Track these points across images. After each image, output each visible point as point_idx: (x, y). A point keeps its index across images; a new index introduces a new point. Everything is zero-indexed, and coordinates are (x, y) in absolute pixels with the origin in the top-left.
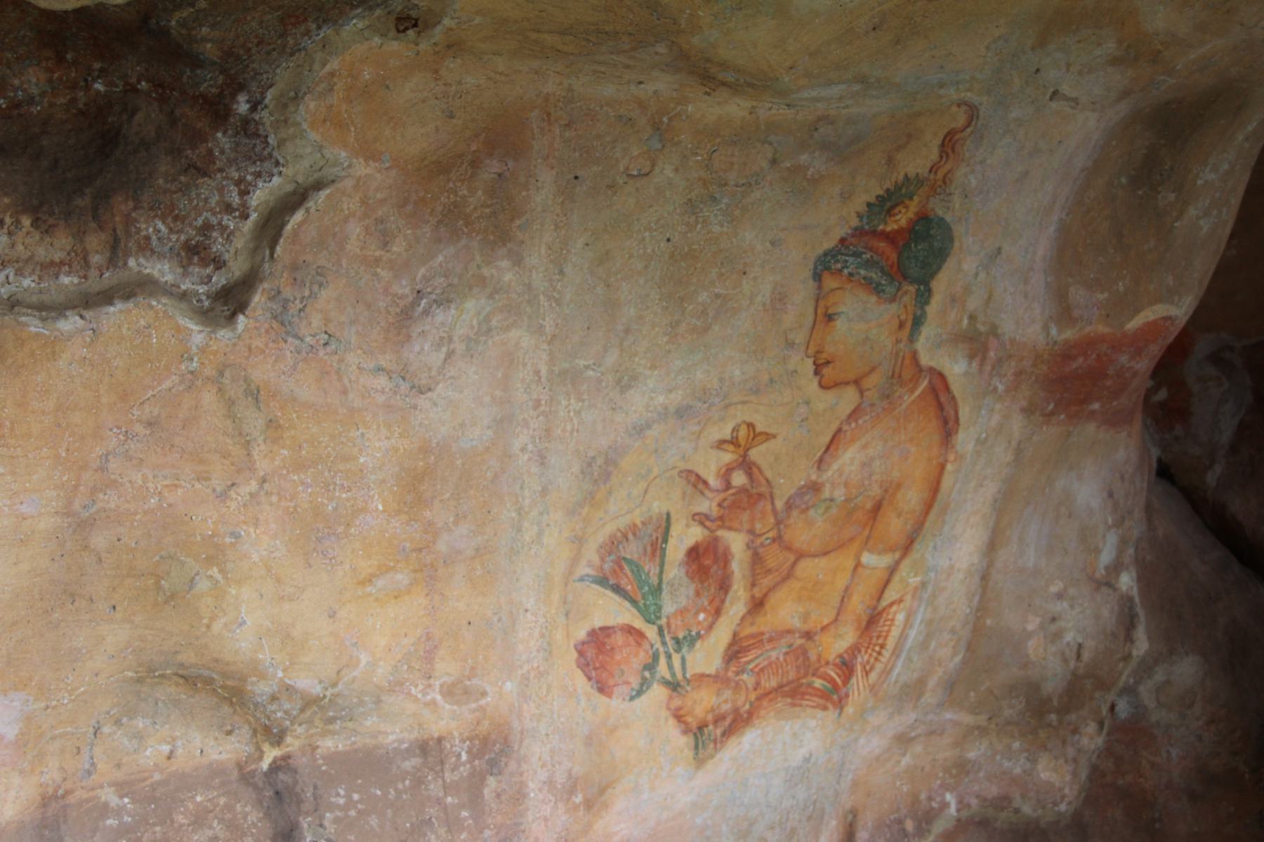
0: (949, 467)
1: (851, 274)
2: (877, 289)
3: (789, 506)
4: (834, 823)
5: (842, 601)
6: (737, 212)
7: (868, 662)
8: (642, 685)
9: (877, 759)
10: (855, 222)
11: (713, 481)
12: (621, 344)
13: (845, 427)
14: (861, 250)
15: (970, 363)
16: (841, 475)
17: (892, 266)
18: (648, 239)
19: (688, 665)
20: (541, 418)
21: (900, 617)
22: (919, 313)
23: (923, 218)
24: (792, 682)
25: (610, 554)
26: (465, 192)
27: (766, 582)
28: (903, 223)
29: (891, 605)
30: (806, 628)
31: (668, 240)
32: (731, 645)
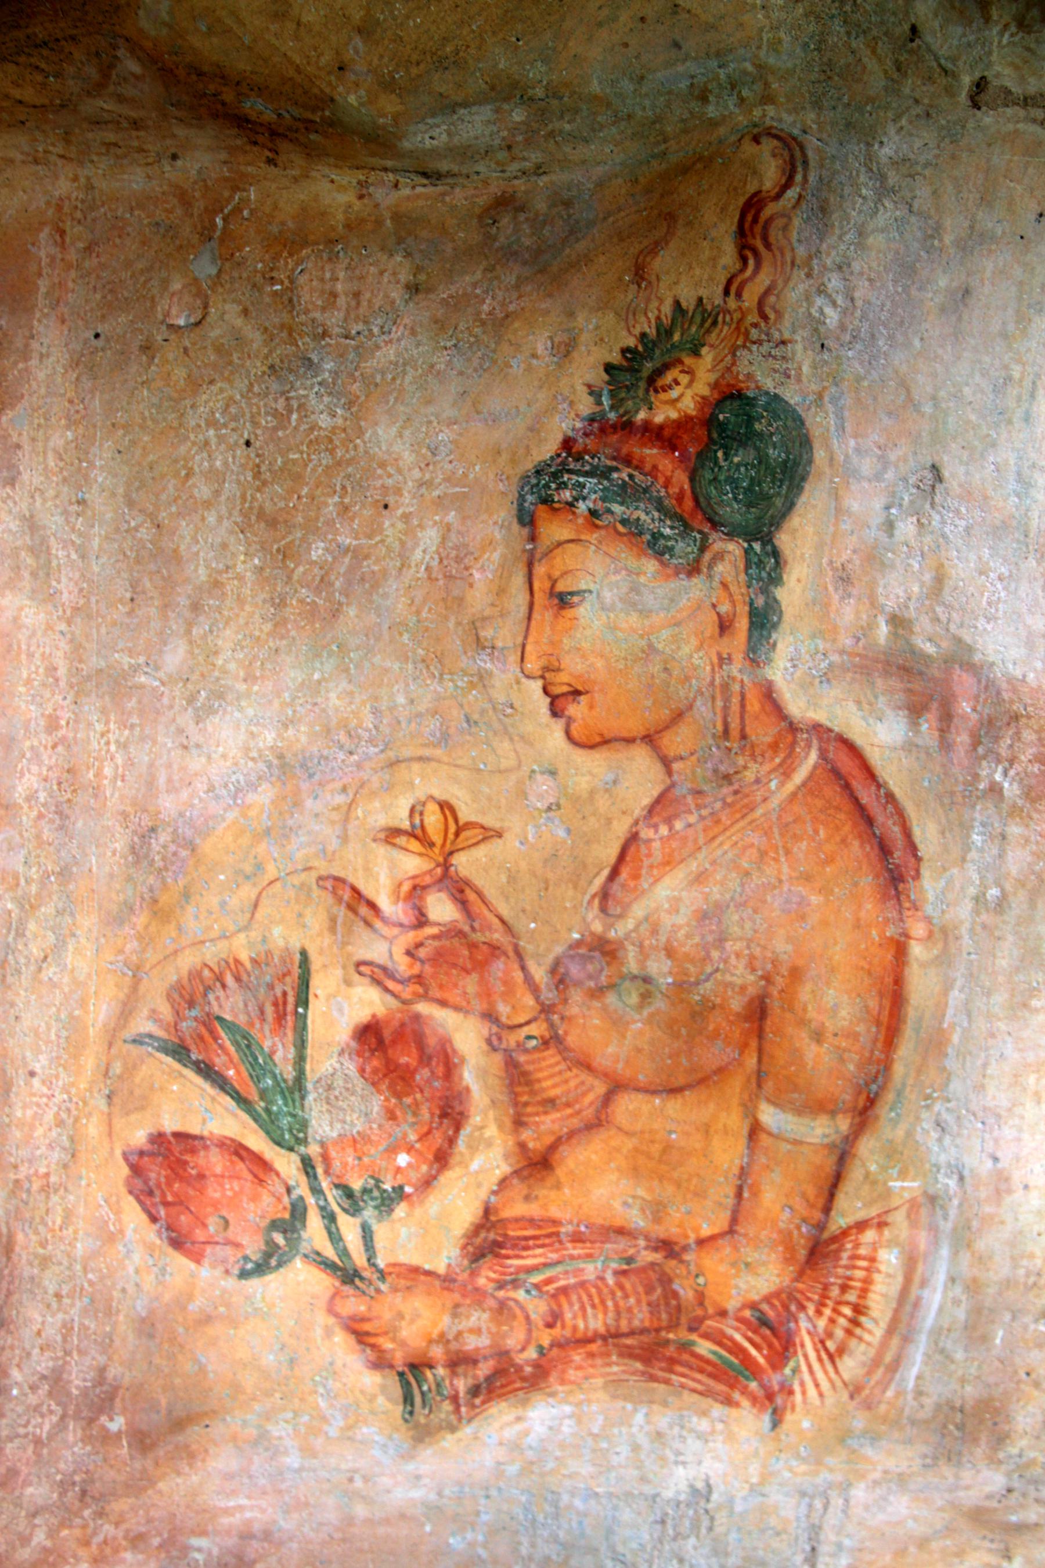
0: (916, 950)
1: (593, 513)
2: (657, 547)
5: (739, 1195)
6: (356, 387)
8: (268, 1255)
10: (586, 406)
11: (384, 903)
12: (188, 632)
13: (646, 833)
17: (680, 498)
18: (213, 441)
20: (60, 749)
22: (760, 601)
23: (731, 395)
24: (643, 1331)
25: (191, 1004)
28: (689, 405)
29: (861, 1226)
30: (660, 1231)
31: (248, 444)
32: (477, 1229)
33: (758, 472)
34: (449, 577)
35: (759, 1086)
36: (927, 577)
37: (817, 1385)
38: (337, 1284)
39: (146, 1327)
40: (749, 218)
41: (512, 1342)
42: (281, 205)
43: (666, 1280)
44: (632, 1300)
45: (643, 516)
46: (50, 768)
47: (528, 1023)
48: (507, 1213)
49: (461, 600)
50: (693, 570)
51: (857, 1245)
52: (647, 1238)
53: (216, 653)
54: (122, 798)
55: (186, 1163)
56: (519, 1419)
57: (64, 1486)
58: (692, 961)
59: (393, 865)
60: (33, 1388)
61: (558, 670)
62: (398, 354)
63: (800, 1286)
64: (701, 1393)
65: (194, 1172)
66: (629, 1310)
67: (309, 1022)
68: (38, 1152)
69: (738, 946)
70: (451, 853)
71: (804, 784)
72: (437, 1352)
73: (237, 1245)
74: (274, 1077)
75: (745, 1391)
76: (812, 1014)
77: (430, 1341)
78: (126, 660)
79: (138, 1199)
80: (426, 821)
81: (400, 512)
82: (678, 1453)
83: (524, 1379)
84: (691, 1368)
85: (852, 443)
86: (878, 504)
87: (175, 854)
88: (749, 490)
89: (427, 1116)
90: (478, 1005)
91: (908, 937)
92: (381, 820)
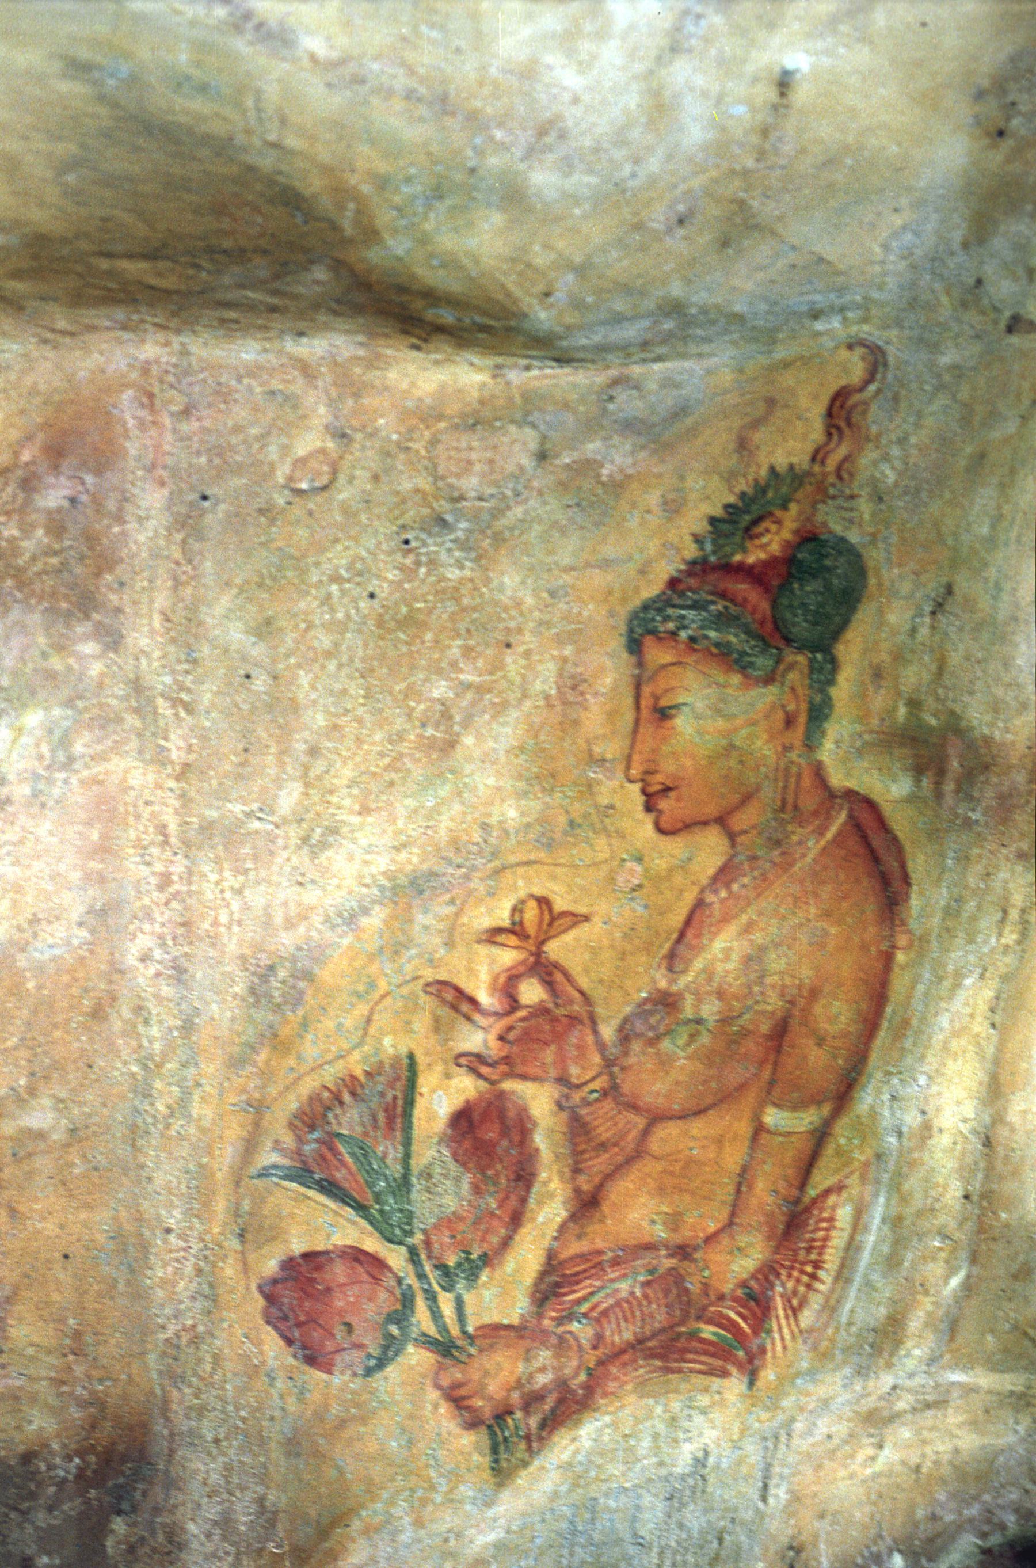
0: (900, 957)
1: (692, 639)
3: (625, 1036)
5: (738, 1191)
7: (795, 1293)
8: (386, 1348)
10: (691, 551)
11: (484, 998)
12: (305, 775)
13: (710, 898)
14: (704, 596)
15: (917, 781)
16: (710, 979)
17: (762, 623)
19: (469, 1310)
20: (174, 905)
22: (818, 699)
24: (663, 1330)
25: (312, 1128)
26: (16, 533)
27: (599, 1164)
28: (775, 548)
29: (827, 1192)
30: (678, 1239)
32: (543, 1275)
34: (565, 703)
35: (769, 1093)
36: (934, 667)
37: (782, 1339)
39: (292, 1445)
40: (838, 404)
42: (420, 383)
46: (163, 925)
47: (593, 1079)
48: (565, 1255)
49: (576, 723)
50: (769, 679)
52: (667, 1247)
54: (240, 941)
55: (312, 1281)
56: (574, 1440)
58: (737, 999)
59: (493, 962)
61: (656, 772)
62: (526, 512)
68: (182, 1307)
70: (543, 942)
77: (509, 1391)
79: (276, 1328)
81: (521, 649)
83: (577, 1402)
84: (697, 1353)
86: (908, 616)
92: (487, 923)
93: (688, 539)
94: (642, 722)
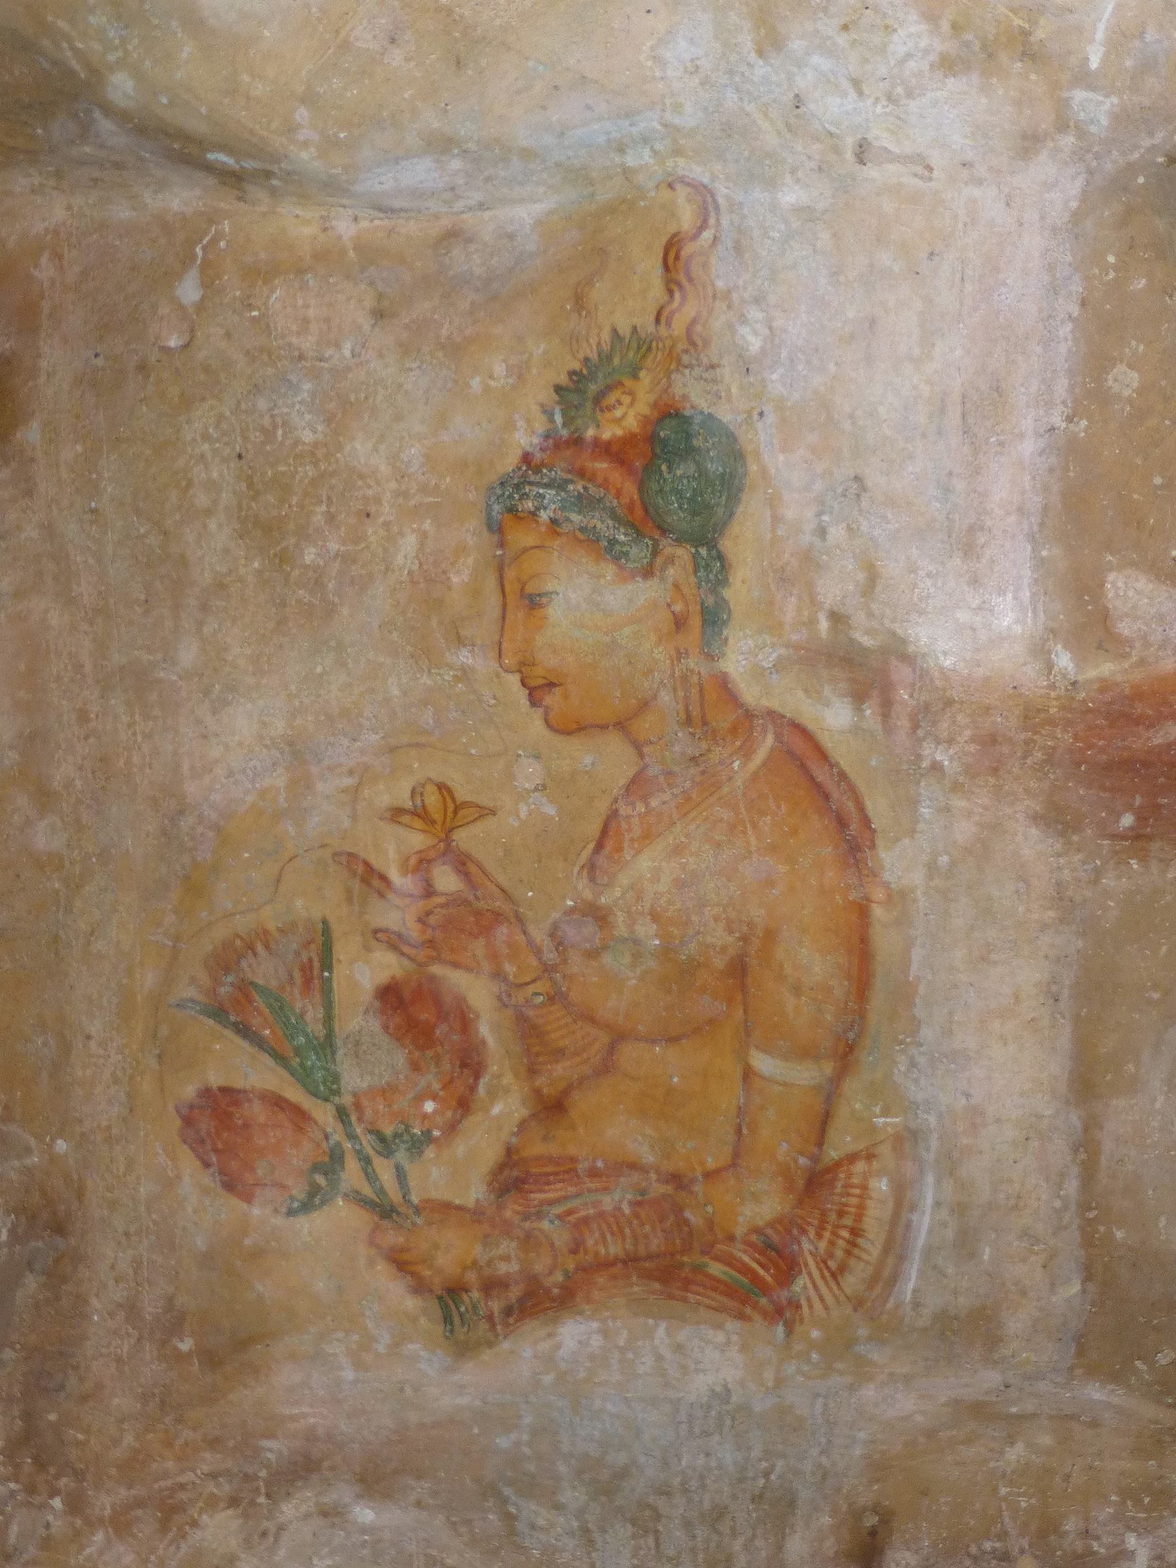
1: (553, 521)
2: (611, 551)
4: (826, 1520)
5: (739, 1131)
8: (312, 1195)
9: (931, 1434)
10: (540, 426)
11: (394, 876)
13: (624, 810)
14: (559, 473)
15: (859, 710)
16: (639, 898)
17: (631, 508)
18: (209, 455)
20: (92, 740)
21: (882, 1185)
23: (669, 413)
25: (227, 970)
27: (561, 1070)
28: (632, 423)
31: (240, 456)
32: (501, 1167)
33: (699, 483)
35: (748, 1033)
36: (861, 576)
37: (822, 1300)
38: (376, 1219)
40: (672, 255)
41: (539, 1267)
43: (678, 1210)
44: (648, 1228)
45: (599, 525)
47: (534, 981)
48: (527, 1153)
50: (648, 572)
51: (850, 1175)
52: (657, 1172)
53: (226, 649)
56: (550, 1335)
57: (145, 1398)
60: (111, 1314)
61: (534, 664)
63: (800, 1212)
64: (716, 1309)
65: (240, 1122)
66: (646, 1236)
67: (335, 986)
69: (716, 911)
71: (764, 764)
72: (471, 1277)
73: (283, 1187)
74: (306, 1035)
75: (755, 1306)
76: (788, 970)
77: (465, 1269)
78: (146, 657)
80: (427, 802)
81: (381, 520)
82: (697, 1362)
83: (553, 1300)
84: (705, 1287)
85: (781, 458)
86: (809, 513)
87: (202, 834)
88: (692, 500)
89: (448, 1067)
90: (486, 966)
91: (868, 900)
92: (385, 800)
93: (535, 408)
94: (509, 607)
